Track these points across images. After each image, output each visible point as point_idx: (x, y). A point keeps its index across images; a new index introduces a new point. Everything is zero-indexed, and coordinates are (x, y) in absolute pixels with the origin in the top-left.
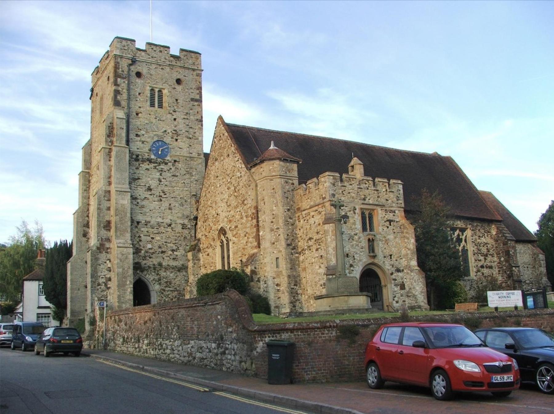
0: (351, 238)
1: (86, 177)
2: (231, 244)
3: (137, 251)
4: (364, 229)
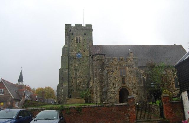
0: (115, 78)
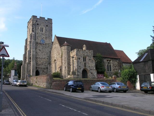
0: (81, 63)
1: (26, 47)
2: (57, 63)
3: (37, 64)
4: (84, 61)
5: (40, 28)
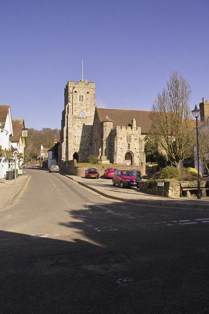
4: (127, 141)
5: (78, 97)
